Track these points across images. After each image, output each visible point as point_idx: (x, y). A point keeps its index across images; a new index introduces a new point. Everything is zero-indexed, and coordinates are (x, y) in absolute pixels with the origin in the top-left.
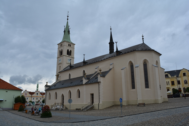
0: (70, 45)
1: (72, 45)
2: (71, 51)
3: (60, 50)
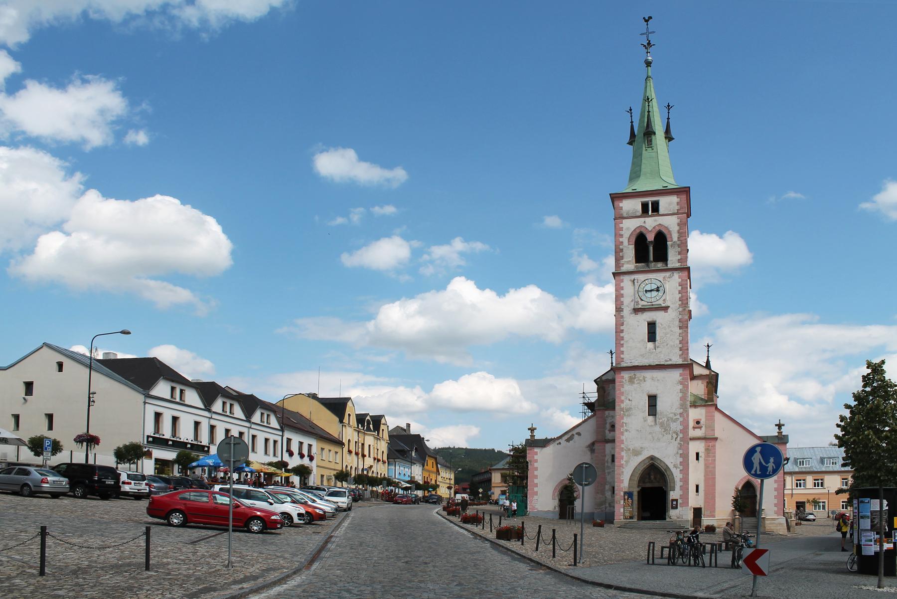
2: (661, 238)
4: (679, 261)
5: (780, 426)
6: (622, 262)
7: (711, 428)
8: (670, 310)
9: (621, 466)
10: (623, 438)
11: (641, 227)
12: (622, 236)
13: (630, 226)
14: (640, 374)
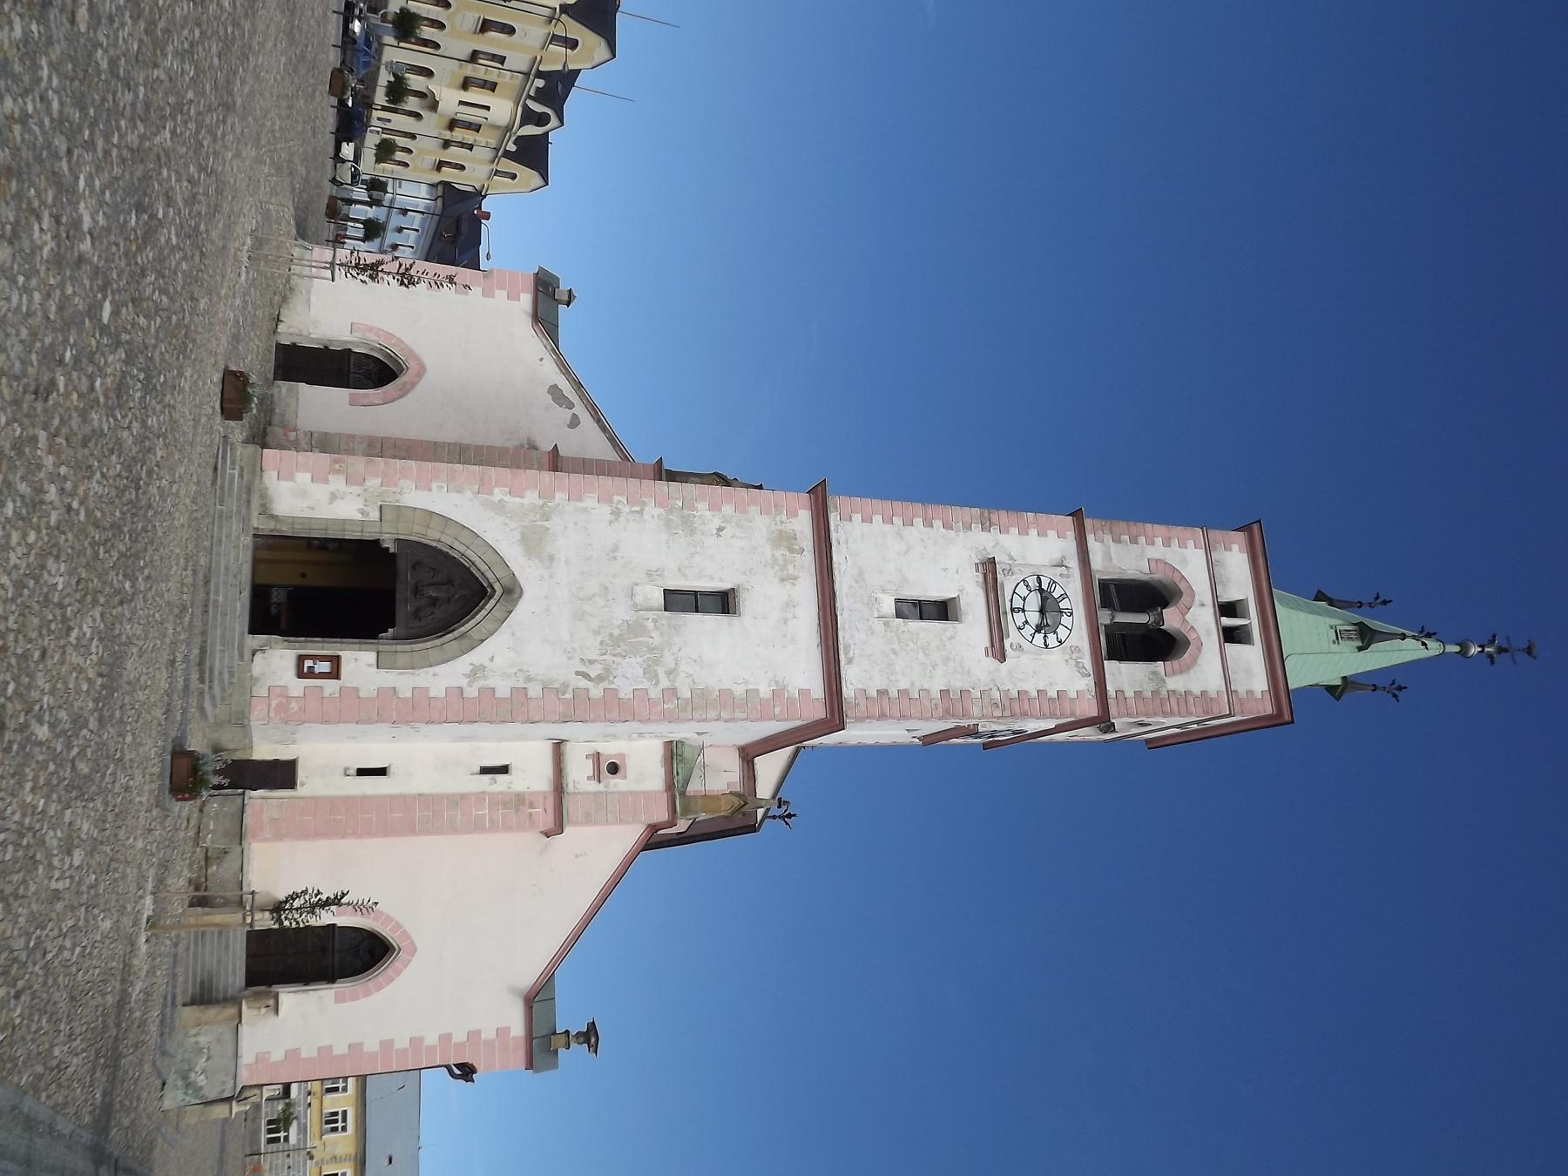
4: (1119, 692)
5: (589, 1036)
7: (601, 810)
8: (991, 662)
9: (484, 487)
10: (590, 501)
14: (806, 562)
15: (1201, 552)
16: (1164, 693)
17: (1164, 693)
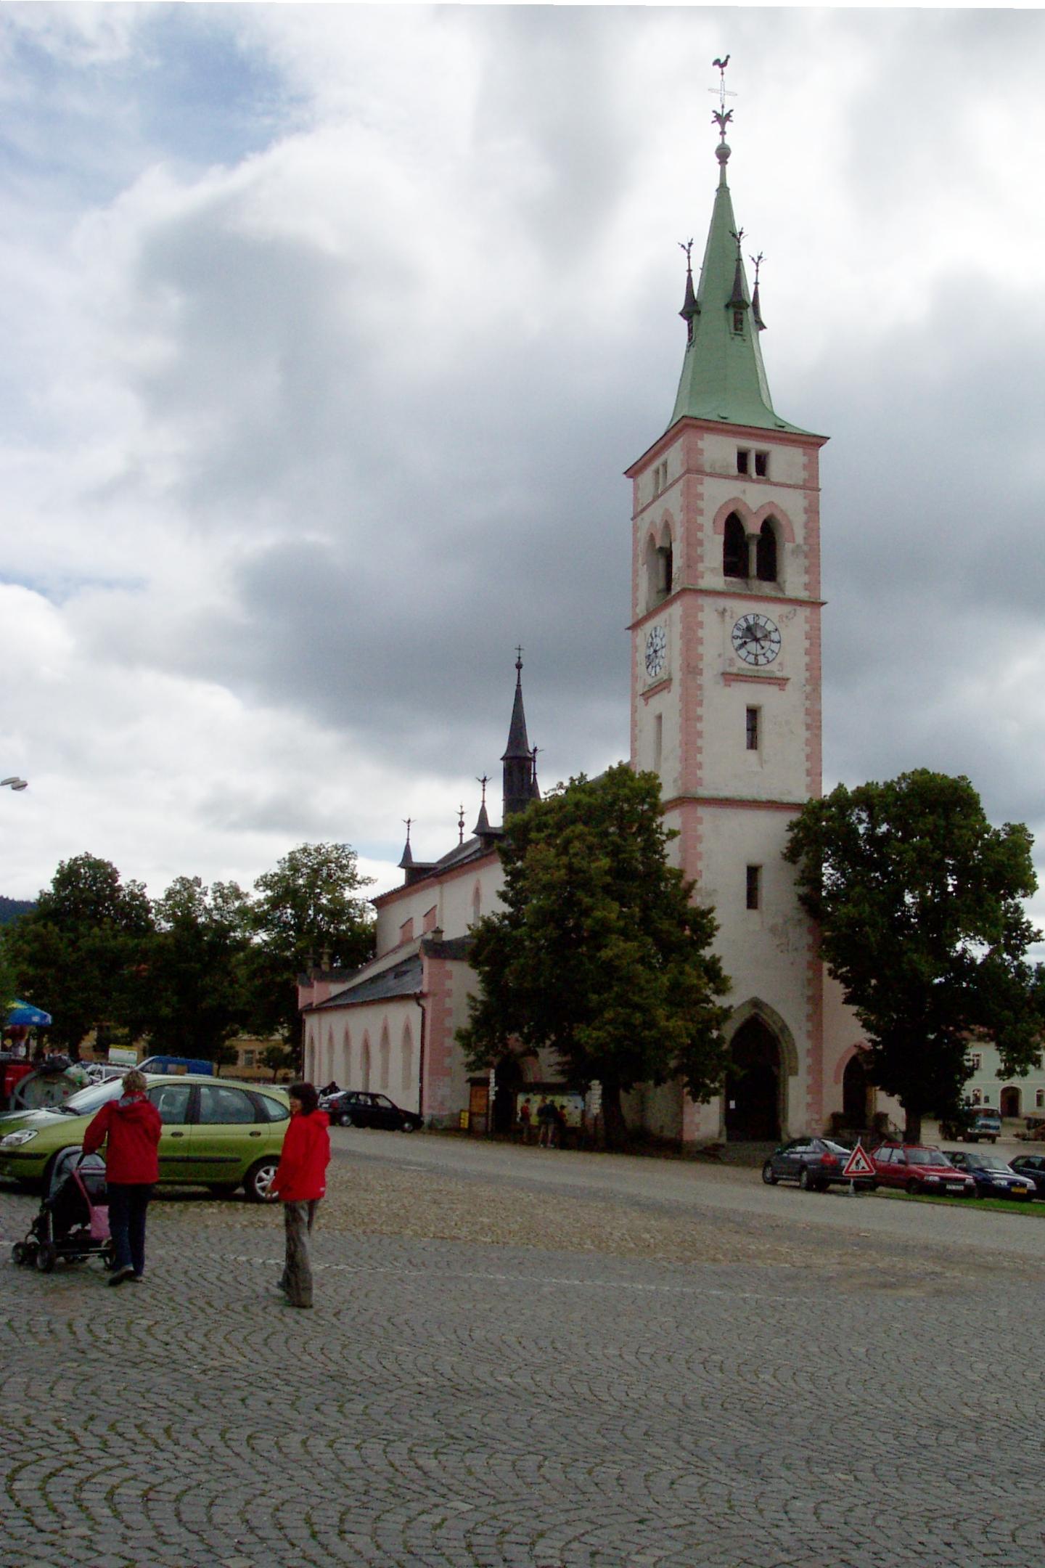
0: (752, 465)
1: (783, 460)
2: (769, 530)
3: (652, 538)
6: (701, 567)
8: (789, 687)
11: (735, 500)
12: (701, 512)
13: (720, 494)
15: (707, 480)
16: (806, 548)
17: (806, 548)
